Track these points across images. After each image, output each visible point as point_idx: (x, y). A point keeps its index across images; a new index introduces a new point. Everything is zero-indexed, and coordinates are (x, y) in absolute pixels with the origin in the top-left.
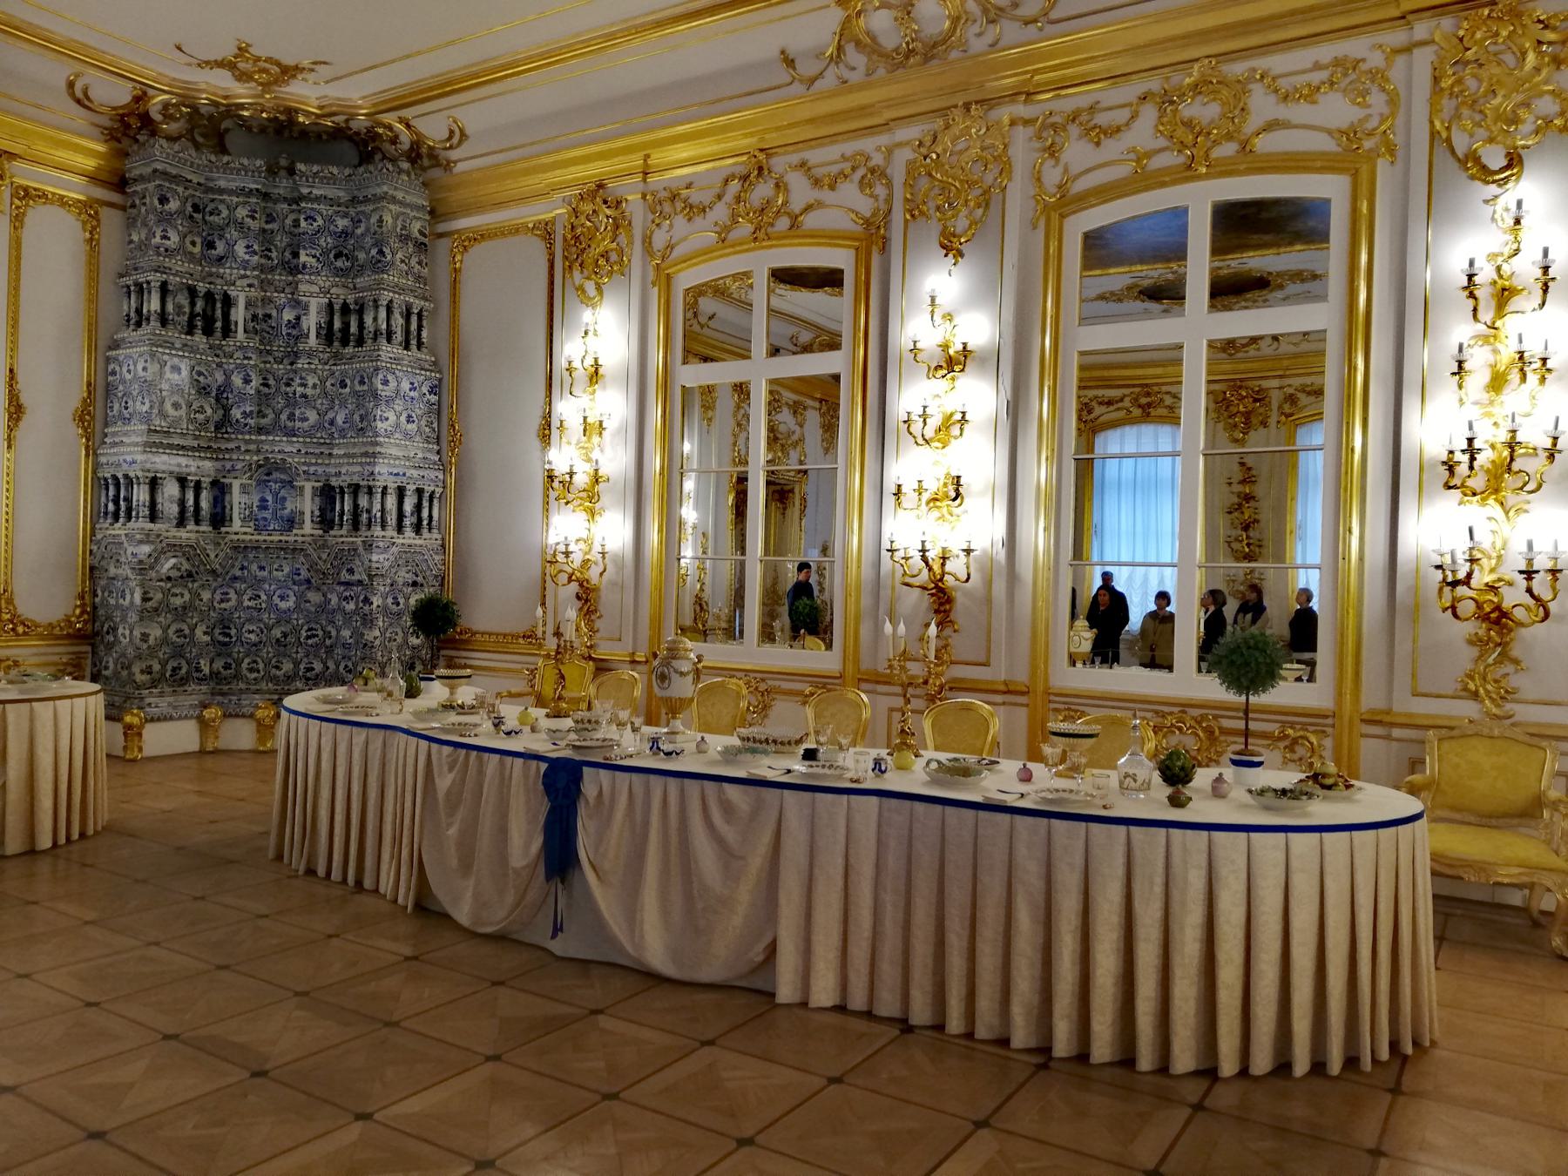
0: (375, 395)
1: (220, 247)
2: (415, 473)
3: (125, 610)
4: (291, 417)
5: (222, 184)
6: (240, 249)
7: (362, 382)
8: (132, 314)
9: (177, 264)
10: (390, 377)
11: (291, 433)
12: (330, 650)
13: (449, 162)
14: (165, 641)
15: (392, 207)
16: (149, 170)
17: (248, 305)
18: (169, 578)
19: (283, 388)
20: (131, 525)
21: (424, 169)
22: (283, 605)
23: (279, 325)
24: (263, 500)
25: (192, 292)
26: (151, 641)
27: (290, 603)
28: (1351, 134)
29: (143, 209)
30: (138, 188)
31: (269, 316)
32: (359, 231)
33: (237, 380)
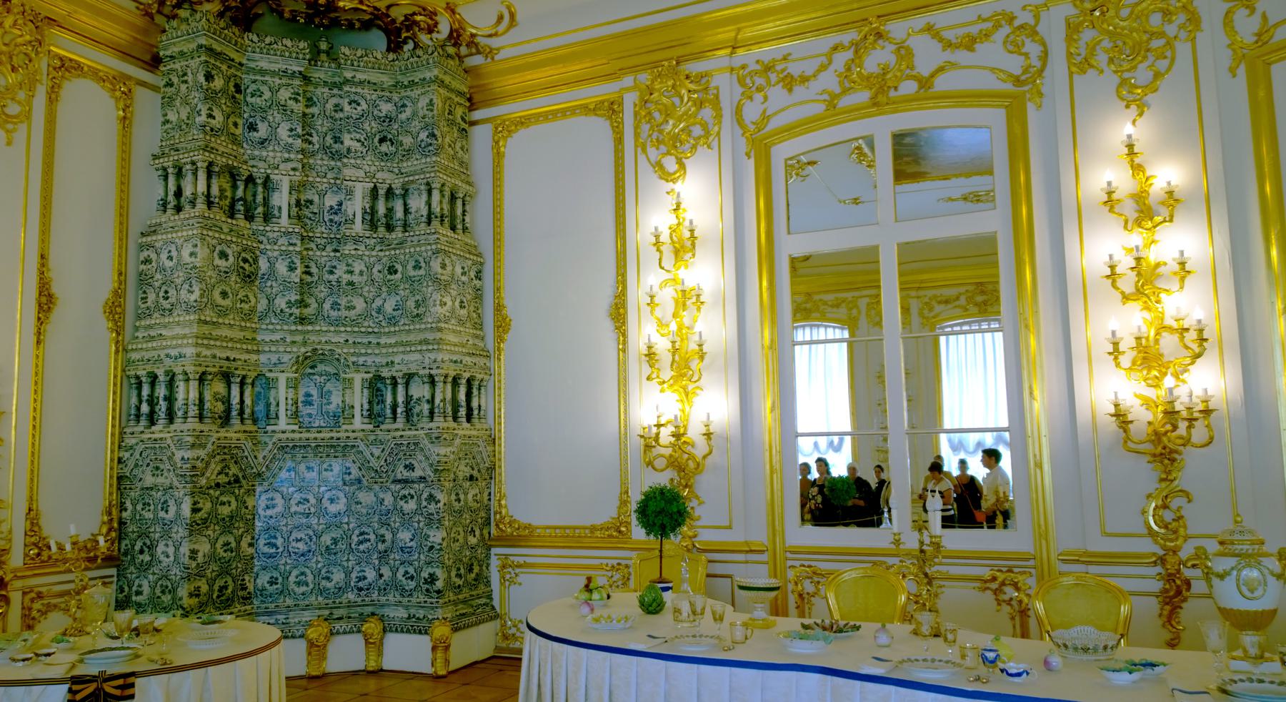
0: (436, 280)
1: (263, 130)
2: (468, 359)
3: (167, 527)
4: (336, 306)
5: (264, 64)
6: (283, 132)
7: (417, 267)
8: (171, 198)
9: (222, 144)
10: (447, 261)
11: (337, 322)
12: (384, 555)
14: (213, 557)
15: (441, 91)
16: (193, 46)
17: (291, 189)
18: (218, 485)
19: (326, 276)
20: (173, 427)
21: (460, 58)
22: (333, 509)
23: (321, 212)
24: (308, 395)
25: (233, 176)
26: (200, 559)
27: (340, 506)
29: (184, 87)
30: (177, 66)
31: (311, 202)
32: (403, 116)
33: (282, 268)
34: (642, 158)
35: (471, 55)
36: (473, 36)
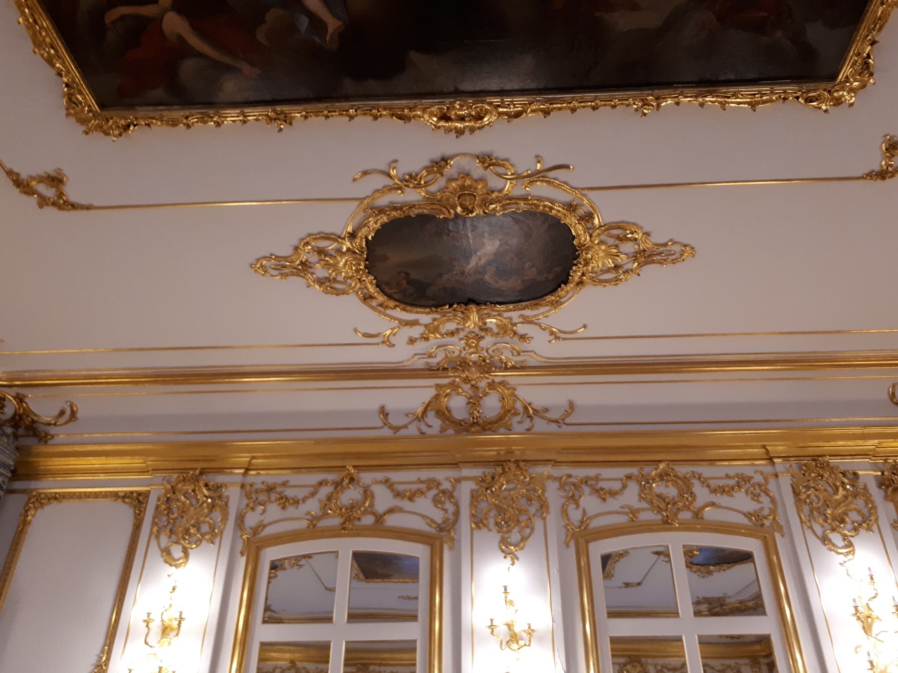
13: (47, 434)
28: (756, 517)
34: (153, 543)
35: (28, 436)
36: (33, 421)
